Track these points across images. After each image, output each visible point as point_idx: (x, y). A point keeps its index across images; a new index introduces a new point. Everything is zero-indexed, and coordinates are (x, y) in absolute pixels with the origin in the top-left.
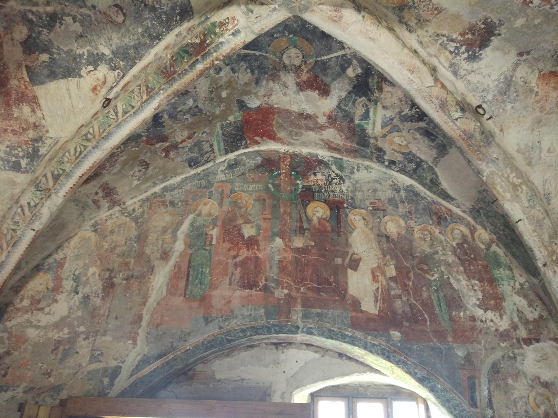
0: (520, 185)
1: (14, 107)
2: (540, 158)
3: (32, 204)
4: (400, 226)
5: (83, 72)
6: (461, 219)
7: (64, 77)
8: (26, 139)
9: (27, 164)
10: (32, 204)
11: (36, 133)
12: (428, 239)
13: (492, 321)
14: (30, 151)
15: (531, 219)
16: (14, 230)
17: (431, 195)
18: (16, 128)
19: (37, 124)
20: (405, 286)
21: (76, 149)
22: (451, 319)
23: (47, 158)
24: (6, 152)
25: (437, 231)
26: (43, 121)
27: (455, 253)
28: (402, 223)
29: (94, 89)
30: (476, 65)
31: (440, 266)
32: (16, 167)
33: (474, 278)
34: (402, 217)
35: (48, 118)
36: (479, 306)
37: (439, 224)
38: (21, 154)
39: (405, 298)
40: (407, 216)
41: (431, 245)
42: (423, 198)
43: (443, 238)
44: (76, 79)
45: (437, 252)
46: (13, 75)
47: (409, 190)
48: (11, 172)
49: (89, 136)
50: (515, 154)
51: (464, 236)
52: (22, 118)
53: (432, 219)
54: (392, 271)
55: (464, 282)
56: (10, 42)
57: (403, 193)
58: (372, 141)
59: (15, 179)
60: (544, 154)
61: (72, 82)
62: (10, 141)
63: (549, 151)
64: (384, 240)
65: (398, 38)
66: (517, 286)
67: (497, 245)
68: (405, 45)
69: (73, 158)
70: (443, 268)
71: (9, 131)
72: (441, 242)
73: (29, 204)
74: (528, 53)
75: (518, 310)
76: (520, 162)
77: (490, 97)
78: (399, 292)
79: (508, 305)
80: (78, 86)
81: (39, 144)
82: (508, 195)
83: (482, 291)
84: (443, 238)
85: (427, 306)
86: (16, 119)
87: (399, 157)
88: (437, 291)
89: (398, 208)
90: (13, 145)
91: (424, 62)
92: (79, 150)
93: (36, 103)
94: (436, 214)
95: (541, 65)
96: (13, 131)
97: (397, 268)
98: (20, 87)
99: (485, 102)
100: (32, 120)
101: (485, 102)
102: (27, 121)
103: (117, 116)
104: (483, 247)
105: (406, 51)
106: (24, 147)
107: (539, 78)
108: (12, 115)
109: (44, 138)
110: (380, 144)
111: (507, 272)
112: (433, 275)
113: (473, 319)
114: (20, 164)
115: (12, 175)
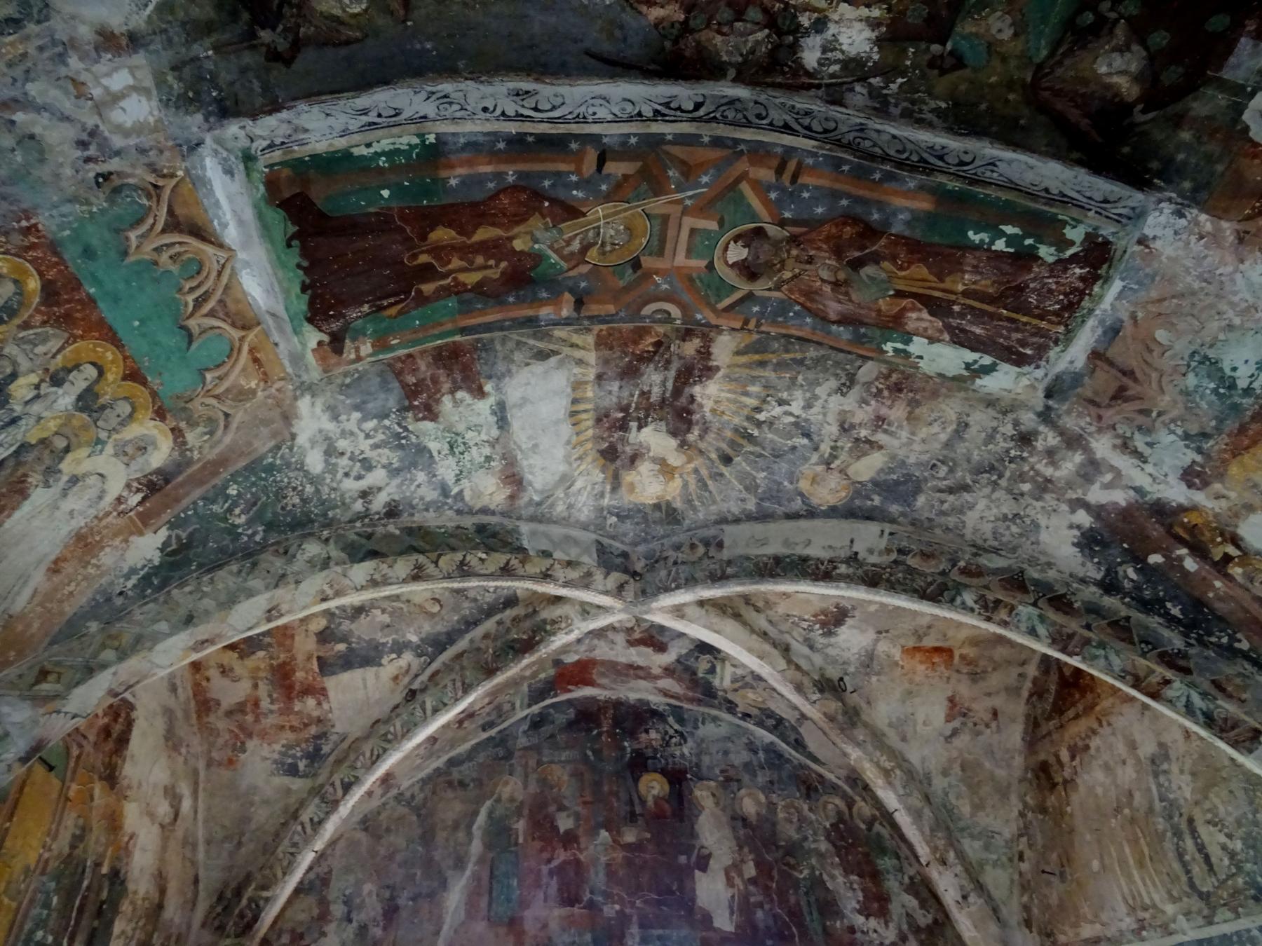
0: (892, 770)
2: (915, 732)
3: (316, 819)
4: (758, 803)
5: (385, 661)
6: (835, 788)
7: (361, 666)
10: (316, 819)
12: (795, 820)
13: (875, 931)
14: (311, 749)
15: (909, 809)
16: (292, 854)
17: (797, 755)
18: (295, 723)
20: (767, 889)
21: (372, 751)
22: (825, 929)
23: (332, 759)
24: (280, 753)
25: (806, 807)
27: (828, 838)
28: (762, 798)
29: (396, 678)
30: (833, 640)
31: (810, 858)
32: (293, 771)
33: (852, 873)
34: (762, 789)
36: (860, 912)
37: (808, 797)
38: (299, 754)
39: (767, 907)
40: (769, 787)
41: (799, 829)
42: (788, 761)
43: (813, 817)
44: (375, 669)
45: (806, 839)
47: (770, 749)
49: (390, 737)
50: (886, 729)
51: (839, 813)
53: (799, 790)
54: (750, 870)
55: (841, 879)
56: (303, 635)
57: (761, 755)
58: (720, 693)
60: (919, 728)
61: (370, 672)
63: (925, 723)
64: (740, 824)
65: (745, 624)
66: (906, 880)
67: (881, 824)
68: (753, 631)
69: (369, 762)
70: (814, 861)
72: (811, 822)
73: (311, 820)
74: (887, 631)
75: (908, 914)
76: (893, 739)
77: (852, 669)
78: (760, 898)
79: (895, 908)
80: (377, 676)
82: (880, 782)
83: (863, 890)
84: (813, 817)
85: (795, 914)
86: (297, 713)
87: (754, 712)
88: (807, 894)
89: (755, 776)
91: (775, 645)
92: (376, 753)
94: (804, 782)
95: (902, 641)
97: (758, 865)
99: (846, 674)
100: (315, 714)
101: (846, 674)
103: (425, 713)
104: (863, 826)
105: (754, 637)
106: (304, 746)
107: (903, 652)
110: (730, 696)
111: (895, 861)
112: (801, 872)
113: (852, 930)
115: (287, 781)
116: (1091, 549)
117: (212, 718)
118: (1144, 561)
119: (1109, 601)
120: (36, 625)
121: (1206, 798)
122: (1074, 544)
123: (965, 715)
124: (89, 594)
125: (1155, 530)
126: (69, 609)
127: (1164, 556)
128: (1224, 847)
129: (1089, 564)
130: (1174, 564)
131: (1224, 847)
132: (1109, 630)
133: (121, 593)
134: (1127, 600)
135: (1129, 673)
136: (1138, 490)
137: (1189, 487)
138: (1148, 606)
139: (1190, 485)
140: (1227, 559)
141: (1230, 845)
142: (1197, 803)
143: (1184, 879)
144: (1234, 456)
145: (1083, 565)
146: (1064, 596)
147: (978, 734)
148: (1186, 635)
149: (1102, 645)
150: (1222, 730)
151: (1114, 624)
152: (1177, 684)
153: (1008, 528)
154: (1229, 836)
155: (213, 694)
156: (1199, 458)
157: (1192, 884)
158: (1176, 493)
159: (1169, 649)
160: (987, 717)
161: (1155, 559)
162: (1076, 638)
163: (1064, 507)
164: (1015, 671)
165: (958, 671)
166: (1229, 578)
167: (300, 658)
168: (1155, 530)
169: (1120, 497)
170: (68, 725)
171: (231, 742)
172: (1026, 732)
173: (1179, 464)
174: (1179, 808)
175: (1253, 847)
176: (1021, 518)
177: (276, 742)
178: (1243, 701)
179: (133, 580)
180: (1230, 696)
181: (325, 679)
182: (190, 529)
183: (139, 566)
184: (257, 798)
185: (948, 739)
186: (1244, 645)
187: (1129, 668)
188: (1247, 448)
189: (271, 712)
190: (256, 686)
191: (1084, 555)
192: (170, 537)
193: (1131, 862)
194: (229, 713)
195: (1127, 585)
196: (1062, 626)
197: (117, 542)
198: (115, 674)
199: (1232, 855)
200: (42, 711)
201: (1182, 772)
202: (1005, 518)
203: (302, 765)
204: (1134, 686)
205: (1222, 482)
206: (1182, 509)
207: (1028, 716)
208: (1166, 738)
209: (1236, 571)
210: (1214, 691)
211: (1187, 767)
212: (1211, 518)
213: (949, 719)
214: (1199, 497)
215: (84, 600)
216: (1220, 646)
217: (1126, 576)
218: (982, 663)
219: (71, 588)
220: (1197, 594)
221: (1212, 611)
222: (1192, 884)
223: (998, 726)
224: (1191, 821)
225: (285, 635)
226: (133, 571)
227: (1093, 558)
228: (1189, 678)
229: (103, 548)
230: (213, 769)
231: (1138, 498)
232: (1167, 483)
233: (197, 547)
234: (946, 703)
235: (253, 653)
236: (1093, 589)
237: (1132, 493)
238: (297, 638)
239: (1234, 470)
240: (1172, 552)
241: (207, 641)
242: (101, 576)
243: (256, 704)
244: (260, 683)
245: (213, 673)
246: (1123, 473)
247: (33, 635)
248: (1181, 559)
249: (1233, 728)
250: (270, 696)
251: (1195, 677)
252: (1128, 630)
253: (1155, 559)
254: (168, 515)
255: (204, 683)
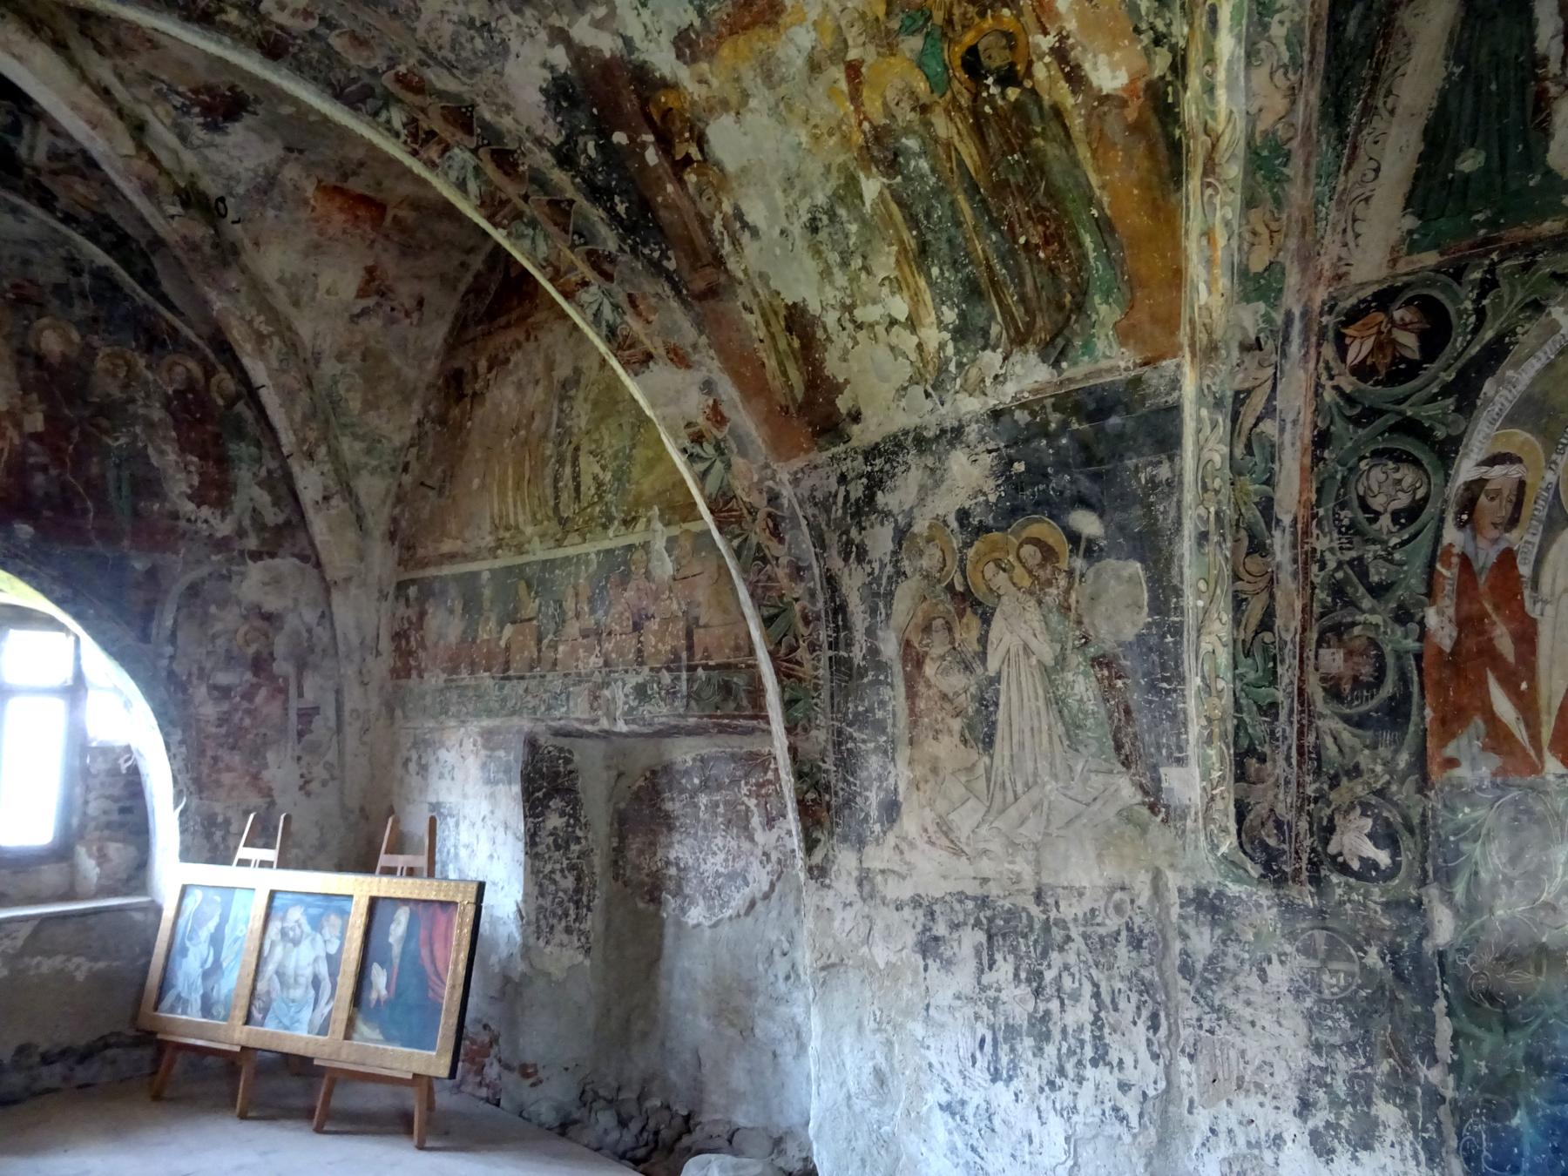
0: (269, 336)
2: (313, 299)
4: (69, 341)
6: (192, 349)
12: (122, 375)
13: (206, 521)
15: (282, 390)
17: (144, 294)
20: (56, 453)
22: (136, 513)
25: (142, 363)
27: (167, 406)
28: (75, 336)
30: (218, 139)
31: (133, 425)
33: (191, 453)
34: (78, 325)
36: (190, 498)
37: (148, 350)
39: (53, 472)
40: (90, 325)
41: (125, 386)
42: (126, 297)
43: (150, 376)
45: (132, 400)
47: (101, 274)
50: (273, 284)
51: (190, 382)
53: (137, 340)
54: (36, 422)
55: (172, 457)
57: (86, 280)
58: (28, 171)
63: (328, 292)
64: (30, 362)
65: (72, 62)
66: (263, 472)
67: (247, 404)
68: (84, 77)
70: (138, 429)
72: (146, 383)
74: (301, 152)
75: (254, 510)
76: (281, 299)
77: (241, 190)
78: (43, 459)
79: (240, 502)
82: (248, 347)
83: (201, 475)
84: (150, 376)
85: (96, 489)
87: (86, 216)
88: (118, 466)
89: (71, 306)
91: (120, 113)
94: (147, 331)
95: (320, 173)
97: (48, 419)
99: (231, 195)
101: (231, 195)
104: (220, 402)
105: (85, 89)
107: (317, 188)
110: (45, 180)
111: (253, 450)
112: (117, 439)
113: (175, 516)
116: (558, 103)
118: (608, 137)
119: (559, 177)
121: (598, 428)
122: (541, 90)
123: (383, 295)
125: (630, 104)
127: (629, 138)
128: (595, 478)
129: (551, 122)
130: (637, 149)
131: (595, 478)
132: (546, 209)
134: (578, 180)
135: (551, 264)
136: (628, 42)
137: (678, 57)
138: (598, 194)
139: (680, 56)
140: (688, 160)
141: (601, 476)
142: (588, 433)
143: (552, 503)
144: (732, 33)
145: (544, 121)
146: (512, 152)
147: (392, 321)
148: (623, 240)
149: (533, 224)
150: (620, 347)
151: (554, 204)
152: (594, 289)
153: (472, 38)
154: (604, 468)
156: (697, 23)
157: (556, 508)
158: (662, 60)
159: (600, 248)
160: (409, 303)
161: (620, 138)
162: (507, 210)
163: (543, 36)
164: (457, 257)
165: (387, 237)
166: (681, 182)
168: (630, 104)
169: (607, 44)
172: (451, 332)
173: (678, 23)
174: (571, 434)
175: (619, 480)
176: (490, 31)
178: (649, 322)
180: (639, 314)
185: (354, 318)
186: (671, 265)
187: (553, 258)
188: (745, 28)
191: (548, 109)
193: (510, 483)
195: (583, 161)
196: (497, 188)
199: (600, 485)
201: (586, 400)
202: (471, 23)
204: (551, 280)
205: (710, 62)
206: (665, 85)
207: (457, 317)
208: (584, 364)
209: (691, 178)
210: (626, 305)
211: (592, 396)
212: (687, 106)
213: (362, 293)
214: (684, 74)
216: (650, 260)
217: (585, 151)
218: (420, 235)
220: (648, 194)
221: (656, 218)
222: (556, 508)
223: (420, 319)
224: (577, 449)
227: (557, 114)
228: (607, 285)
231: (625, 52)
232: (658, 43)
234: (362, 273)
236: (546, 155)
237: (620, 42)
239: (725, 51)
240: (639, 134)
246: (619, 11)
248: (644, 146)
249: (631, 347)
251: (614, 287)
252: (567, 214)
253: (620, 138)
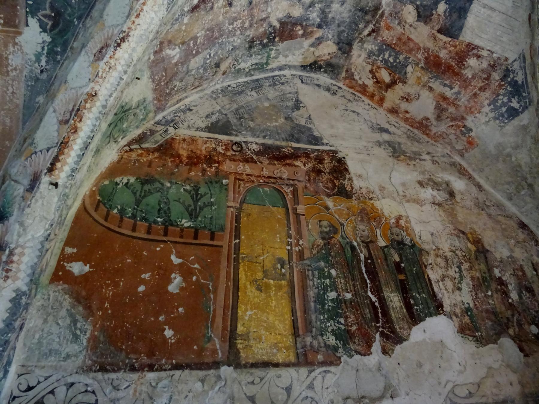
1: (463, 71)
8: (497, 84)
9: (519, 103)
11: (499, 71)
14: (509, 89)
18: (481, 84)
19: (492, 63)
23: (529, 79)
24: (492, 111)
26: (495, 55)
32: (513, 113)
35: (496, 49)
38: (505, 100)
46: (437, 49)
48: (513, 121)
52: (477, 72)
56: (412, 29)
59: (522, 124)
62: (487, 98)
71: (479, 92)
81: (512, 76)
86: (474, 77)
90: (492, 99)
93: (473, 49)
96: (480, 89)
98: (450, 52)
100: (485, 65)
102: (482, 71)
106: (502, 91)
108: (467, 78)
109: (509, 67)
114: (513, 107)
115: (516, 122)
117: (434, 130)
120: (8, 121)
124: (23, 85)
126: (20, 101)
133: (42, 71)
155: (419, 118)
167: (430, 44)
170: (47, 158)
171: (458, 132)
177: (482, 107)
179: (44, 60)
181: (461, 38)
182: (48, 5)
183: (39, 50)
184: (508, 150)
189: (459, 93)
190: (431, 89)
192: (39, 20)
194: (439, 118)
197: (11, 49)
198: (54, 111)
200: (23, 158)
203: (515, 104)
215: (23, 90)
219: (11, 90)
225: (404, 44)
226: (38, 57)
229: (7, 58)
230: (466, 155)
233: (66, 9)
235: (406, 73)
238: (412, 37)
241: (102, 48)
242: (21, 72)
243: (445, 98)
244: (431, 85)
245: (404, 106)
247: (11, 127)
250: (445, 85)
254: (21, 11)
255: (408, 116)
